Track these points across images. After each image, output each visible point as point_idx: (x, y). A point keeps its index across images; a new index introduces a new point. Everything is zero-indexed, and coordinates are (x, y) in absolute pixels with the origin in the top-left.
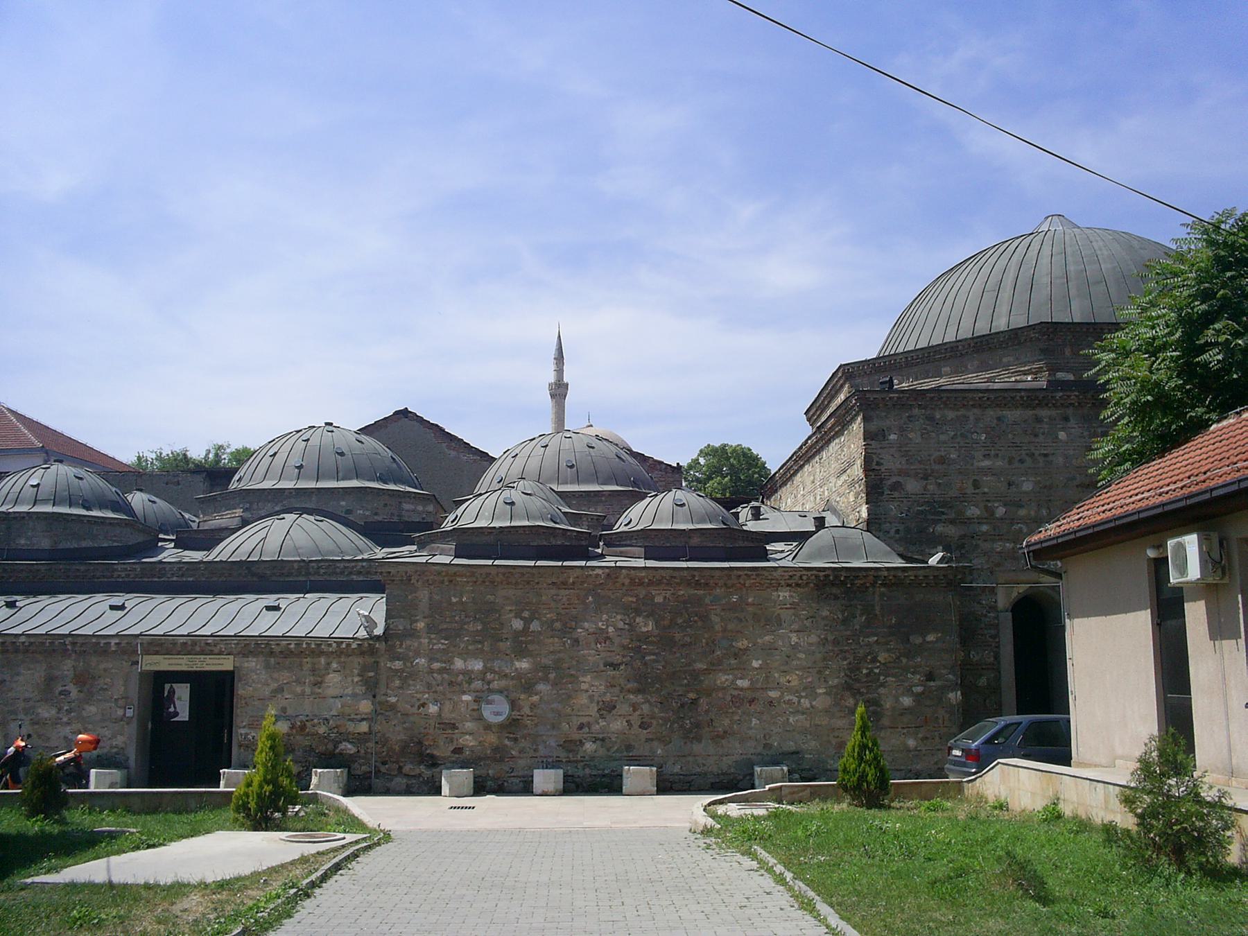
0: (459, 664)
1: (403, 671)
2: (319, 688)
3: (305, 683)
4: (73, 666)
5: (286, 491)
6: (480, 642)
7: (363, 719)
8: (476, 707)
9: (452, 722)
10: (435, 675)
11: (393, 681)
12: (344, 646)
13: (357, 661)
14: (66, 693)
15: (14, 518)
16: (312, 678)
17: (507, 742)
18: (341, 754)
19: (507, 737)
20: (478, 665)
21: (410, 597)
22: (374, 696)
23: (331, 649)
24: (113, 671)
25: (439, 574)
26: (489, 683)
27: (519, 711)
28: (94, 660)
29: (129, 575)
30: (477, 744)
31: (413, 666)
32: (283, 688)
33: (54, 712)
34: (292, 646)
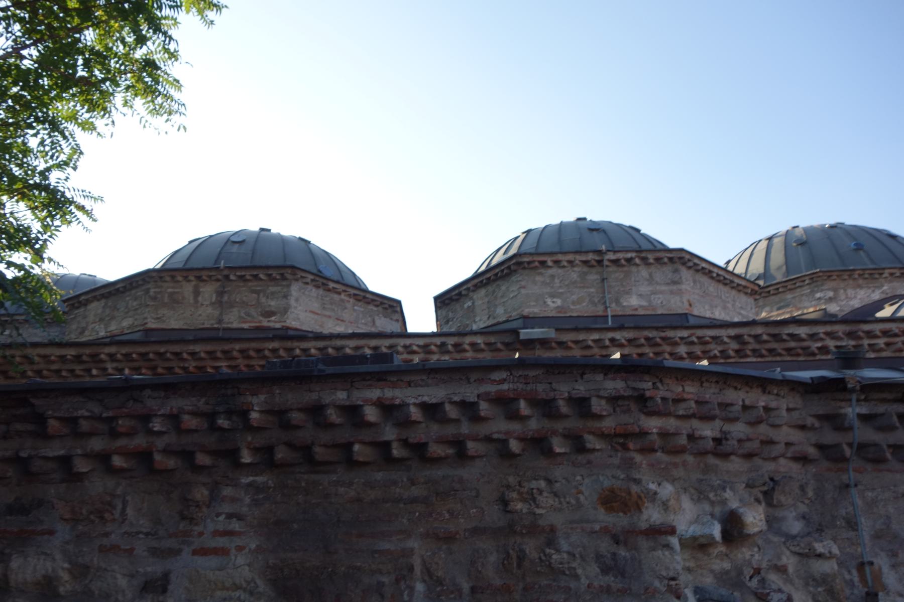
15: (616, 262)
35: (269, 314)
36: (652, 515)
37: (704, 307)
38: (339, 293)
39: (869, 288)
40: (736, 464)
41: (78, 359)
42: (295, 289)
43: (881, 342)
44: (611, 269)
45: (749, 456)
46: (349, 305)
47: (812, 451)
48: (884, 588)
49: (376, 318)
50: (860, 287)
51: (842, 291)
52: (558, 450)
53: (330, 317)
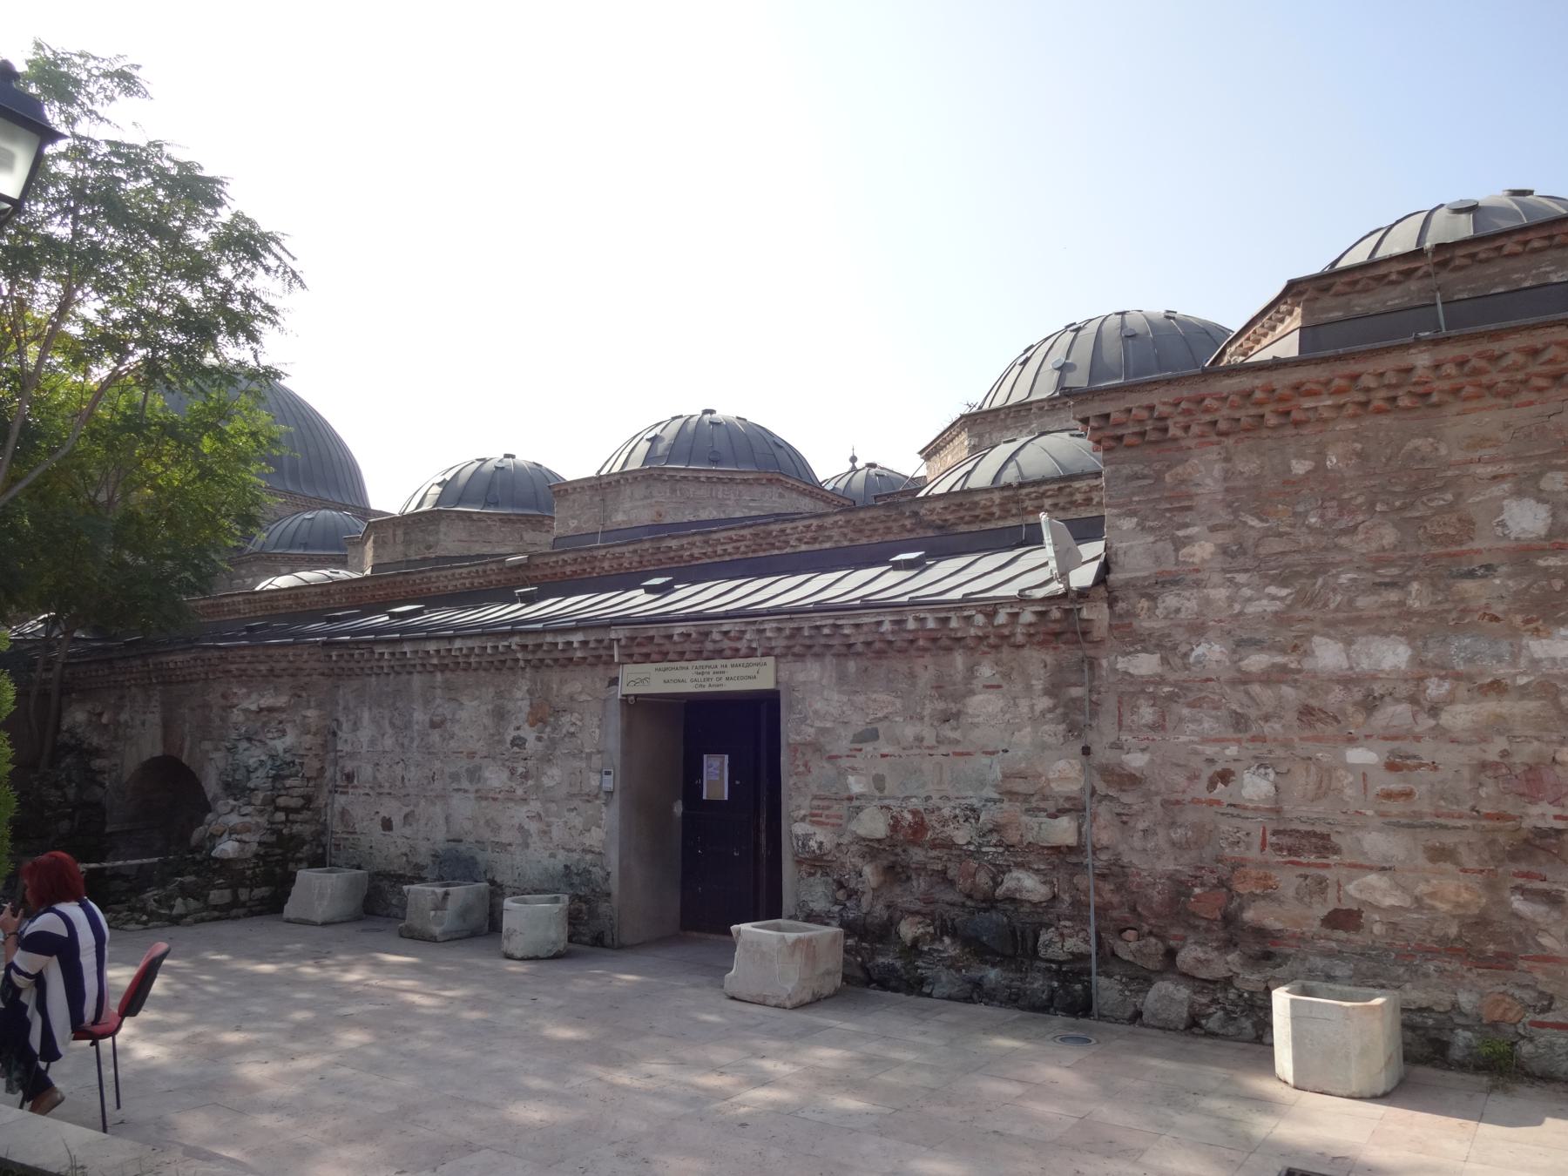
0: (1328, 655)
1: (1160, 680)
2: (956, 729)
3: (922, 718)
4: (528, 691)
5: (1033, 406)
6: (1392, 585)
7: (1062, 812)
8: (1396, 786)
9: (1318, 829)
10: (1256, 688)
11: (1134, 709)
12: (1001, 618)
13: (1038, 663)
14: (518, 742)
15: (610, 483)
16: (941, 705)
17: (1518, 903)
18: (1011, 900)
19: (1519, 889)
20: (1393, 656)
21: (1168, 478)
22: (1086, 751)
23: (973, 632)
24: (583, 697)
25: (1248, 395)
26: (1434, 711)
27: (1555, 802)
28: (554, 677)
29: (738, 548)
30: (1407, 902)
31: (1186, 667)
32: (876, 730)
33: (505, 775)
34: (887, 627)
35: (429, 547)
36: (235, 701)
37: (683, 513)
38: (485, 521)
39: (1016, 428)
40: (285, 679)
41: (322, 594)
42: (443, 528)
43: (729, 548)
44: (608, 491)
45: (292, 675)
46: (494, 528)
47: (326, 671)
48: (341, 731)
49: (524, 533)
50: (1007, 428)
51: (987, 435)
52: (211, 677)
53: (477, 541)
